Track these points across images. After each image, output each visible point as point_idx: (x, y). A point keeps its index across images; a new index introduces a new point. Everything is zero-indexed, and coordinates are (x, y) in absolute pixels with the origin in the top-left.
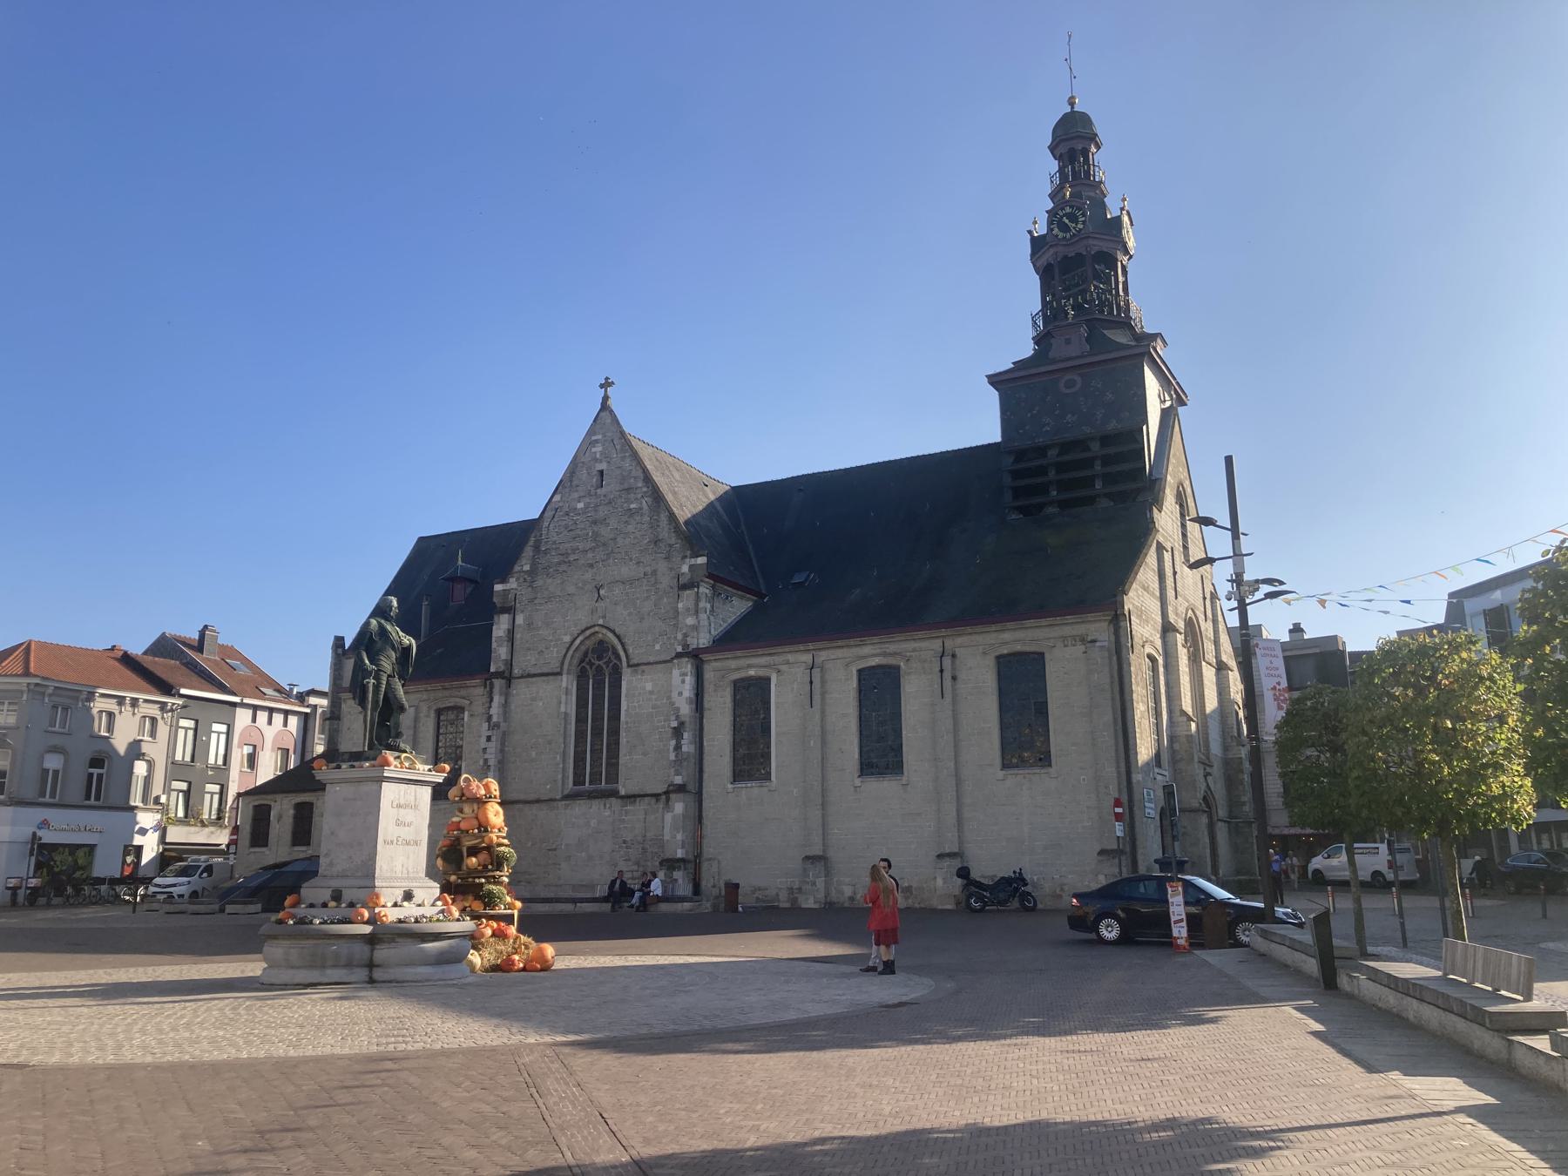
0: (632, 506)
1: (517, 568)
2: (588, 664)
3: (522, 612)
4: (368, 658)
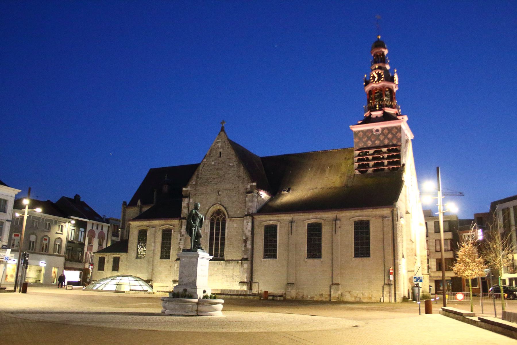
0: (231, 164)
1: (190, 183)
3: (192, 198)
4: (192, 221)
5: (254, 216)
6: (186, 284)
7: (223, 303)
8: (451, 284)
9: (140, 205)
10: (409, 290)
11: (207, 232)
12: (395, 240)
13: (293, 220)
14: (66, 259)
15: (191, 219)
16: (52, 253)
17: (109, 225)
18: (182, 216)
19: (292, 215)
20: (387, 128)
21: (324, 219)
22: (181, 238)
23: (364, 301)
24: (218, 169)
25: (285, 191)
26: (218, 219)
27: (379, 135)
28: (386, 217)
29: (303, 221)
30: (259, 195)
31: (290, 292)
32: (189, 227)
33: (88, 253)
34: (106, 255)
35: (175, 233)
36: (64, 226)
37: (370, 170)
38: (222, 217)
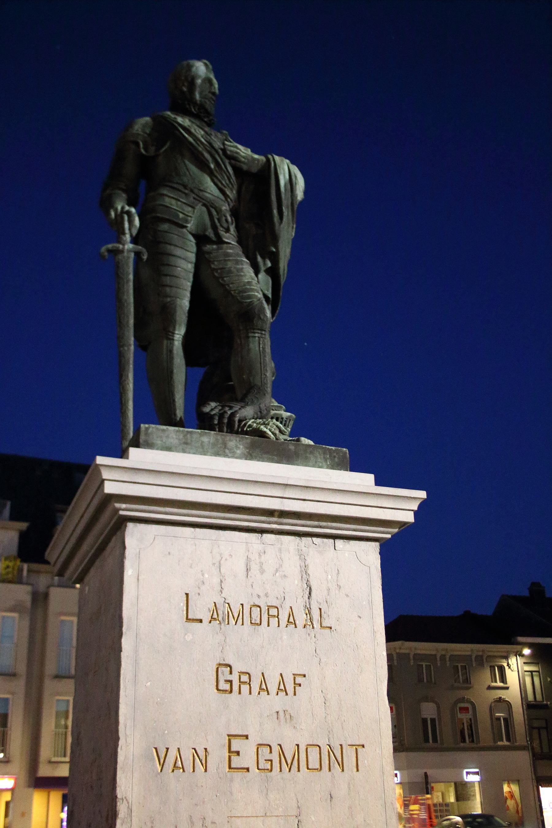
14: (534, 755)
36: (507, 668)
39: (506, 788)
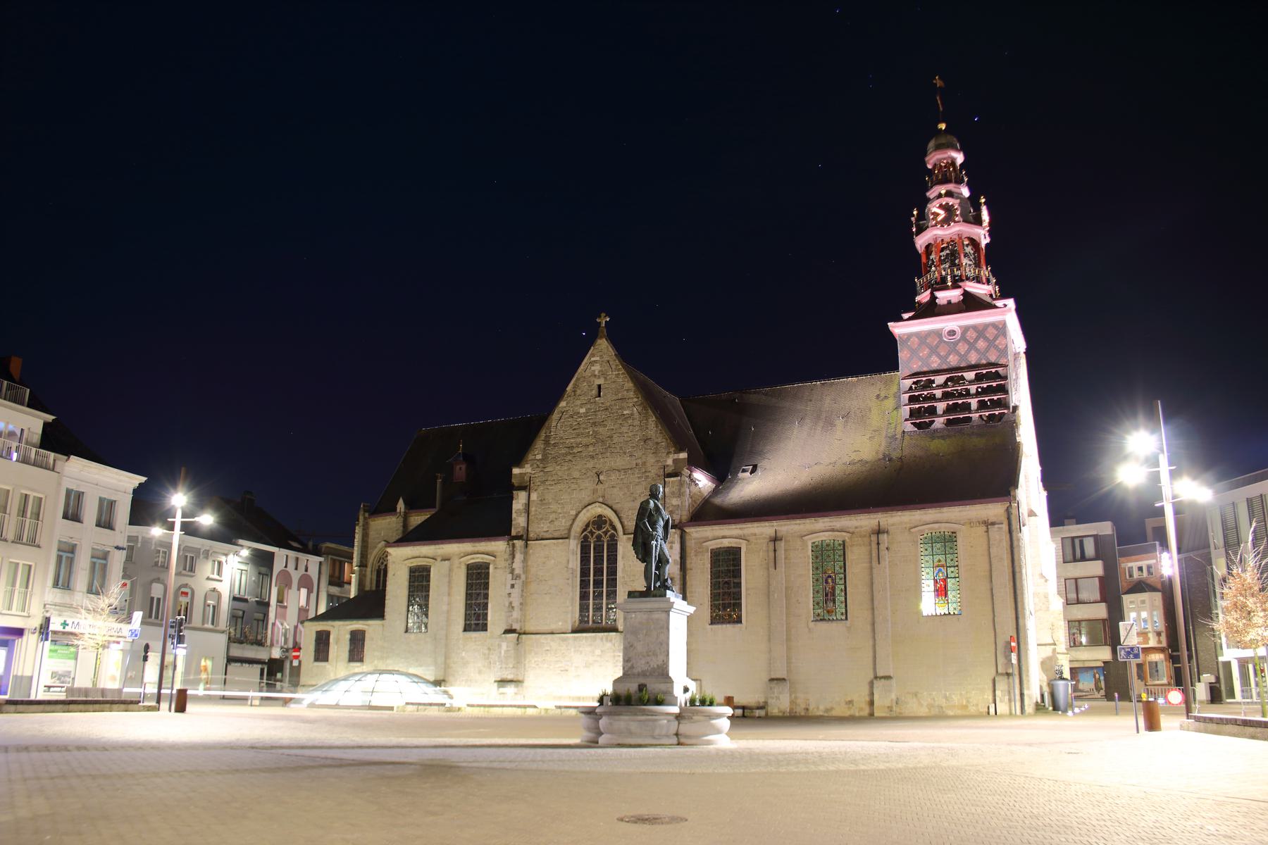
0: (625, 412)
1: (530, 457)
2: (589, 532)
5: (685, 529)
6: (644, 674)
7: (730, 715)
8: (1104, 675)
9: (403, 510)
10: (1041, 688)
11: (575, 568)
12: (1017, 576)
13: (778, 534)
14: (229, 638)
15: (646, 520)
16: (199, 625)
17: (321, 559)
18: (513, 533)
19: (775, 523)
20: (974, 327)
21: (851, 530)
22: (513, 582)
23: (951, 713)
24: (594, 424)
25: (744, 471)
26: (599, 537)
27: (956, 344)
28: (993, 524)
29: (802, 536)
30: (693, 481)
31: (778, 698)
32: (640, 541)
33: (278, 623)
34: (333, 626)
35: (498, 571)
36: (224, 563)
37: (939, 422)
38: (609, 533)
39: (203, 663)
